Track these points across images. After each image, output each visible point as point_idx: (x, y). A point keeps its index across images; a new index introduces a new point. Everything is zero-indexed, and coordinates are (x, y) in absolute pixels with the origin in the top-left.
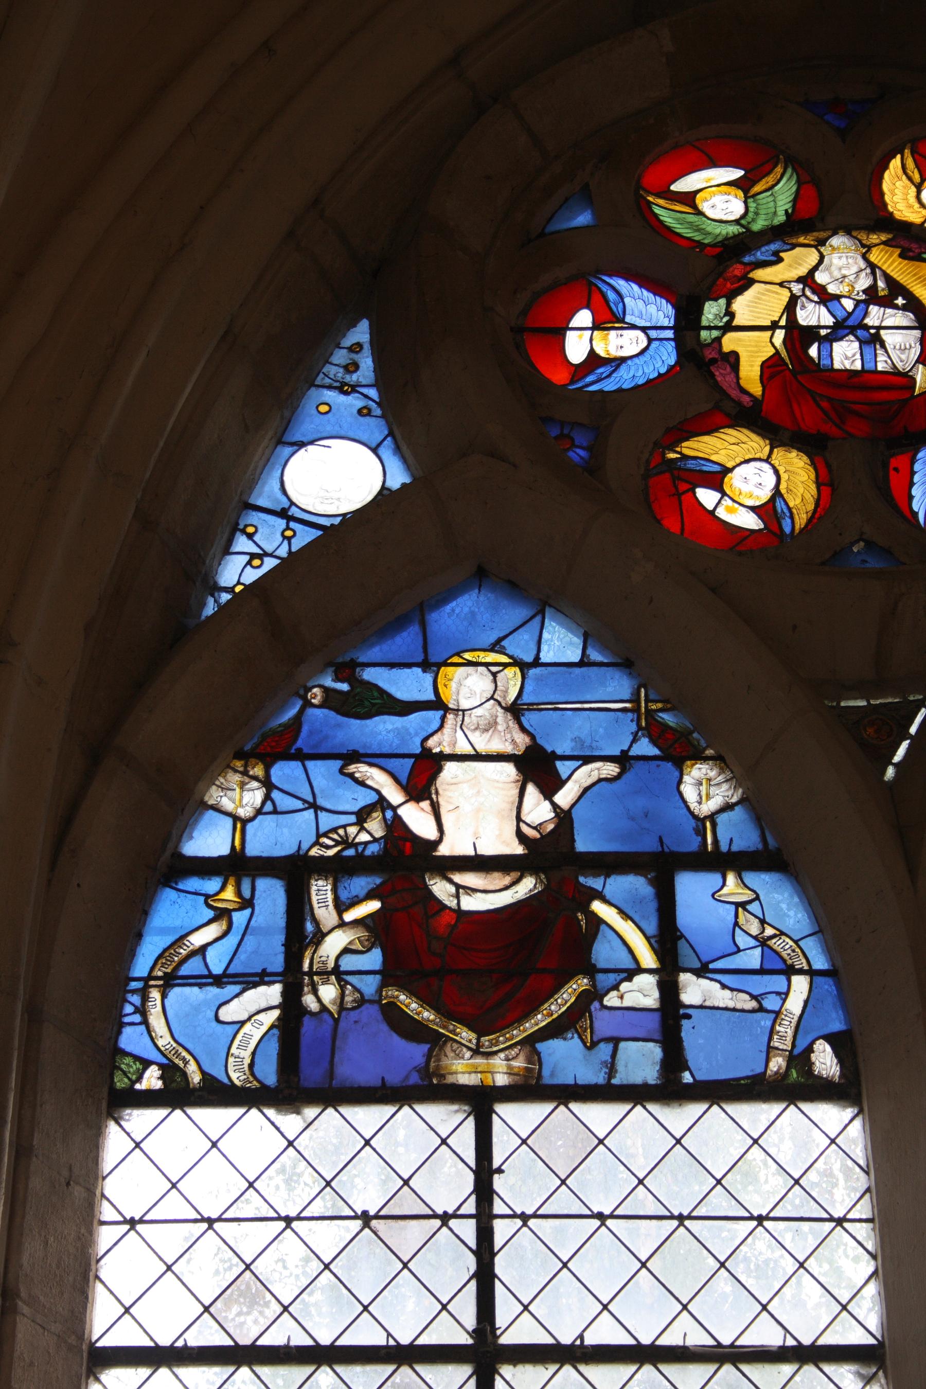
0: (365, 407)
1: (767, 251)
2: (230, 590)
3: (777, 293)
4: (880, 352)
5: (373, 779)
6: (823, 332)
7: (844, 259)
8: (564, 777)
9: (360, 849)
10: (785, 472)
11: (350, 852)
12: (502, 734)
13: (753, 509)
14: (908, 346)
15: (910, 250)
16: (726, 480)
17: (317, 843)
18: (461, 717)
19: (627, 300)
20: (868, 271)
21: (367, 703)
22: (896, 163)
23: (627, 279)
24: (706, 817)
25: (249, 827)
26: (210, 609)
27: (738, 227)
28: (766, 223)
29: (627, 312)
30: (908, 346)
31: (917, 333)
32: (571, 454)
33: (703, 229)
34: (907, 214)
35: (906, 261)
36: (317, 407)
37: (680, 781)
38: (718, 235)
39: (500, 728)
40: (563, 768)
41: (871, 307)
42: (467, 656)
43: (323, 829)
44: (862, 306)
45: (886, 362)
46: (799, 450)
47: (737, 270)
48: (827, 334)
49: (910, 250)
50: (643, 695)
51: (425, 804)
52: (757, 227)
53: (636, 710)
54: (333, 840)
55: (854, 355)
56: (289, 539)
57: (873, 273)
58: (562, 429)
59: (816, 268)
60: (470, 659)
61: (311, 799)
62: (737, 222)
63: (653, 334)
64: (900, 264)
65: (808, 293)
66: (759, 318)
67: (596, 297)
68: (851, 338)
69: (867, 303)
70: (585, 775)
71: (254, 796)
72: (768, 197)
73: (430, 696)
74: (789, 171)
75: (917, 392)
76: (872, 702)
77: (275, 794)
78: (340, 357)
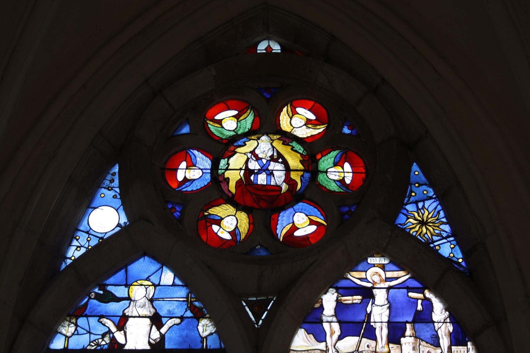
0: (115, 195)
1: (242, 141)
2: (70, 258)
3: (243, 157)
4: (272, 178)
5: (107, 323)
6: (256, 171)
7: (265, 144)
8: (164, 323)
9: (102, 346)
10: (240, 220)
11: (99, 348)
12: (147, 308)
13: (229, 232)
14: (281, 176)
15: (286, 142)
16: (222, 222)
17: (89, 345)
18: (135, 303)
19: (198, 159)
20: (272, 149)
21: (108, 298)
22: (285, 109)
23: (198, 151)
24: (204, 337)
25: (70, 339)
26: (63, 266)
27: (234, 132)
28: (242, 131)
29: (197, 163)
30: (281, 176)
31: (285, 172)
32: (175, 214)
33: (223, 133)
34: (286, 128)
35: (284, 146)
36: (100, 195)
37: (198, 325)
38: (227, 135)
39: (146, 306)
40: (164, 320)
41: (271, 162)
42: (139, 282)
43: (92, 340)
44: (268, 162)
45: (274, 182)
46: (245, 212)
47: (232, 148)
48: (257, 172)
49: (285, 141)
50: (190, 296)
51: (122, 332)
52: (239, 133)
53: (187, 301)
54: (94, 344)
55: (264, 179)
56: (89, 241)
57: (273, 150)
58: (173, 205)
59: (256, 148)
60: (140, 283)
61: (89, 330)
62: (234, 131)
63: (204, 171)
64: (282, 146)
65: (253, 157)
66: (237, 166)
67: (188, 157)
68: (264, 173)
69: (270, 161)
70: (170, 323)
71: (72, 329)
72: (244, 121)
73: (126, 296)
74: (252, 111)
75: (282, 192)
76: (258, 299)
77: (78, 328)
78: (109, 177)
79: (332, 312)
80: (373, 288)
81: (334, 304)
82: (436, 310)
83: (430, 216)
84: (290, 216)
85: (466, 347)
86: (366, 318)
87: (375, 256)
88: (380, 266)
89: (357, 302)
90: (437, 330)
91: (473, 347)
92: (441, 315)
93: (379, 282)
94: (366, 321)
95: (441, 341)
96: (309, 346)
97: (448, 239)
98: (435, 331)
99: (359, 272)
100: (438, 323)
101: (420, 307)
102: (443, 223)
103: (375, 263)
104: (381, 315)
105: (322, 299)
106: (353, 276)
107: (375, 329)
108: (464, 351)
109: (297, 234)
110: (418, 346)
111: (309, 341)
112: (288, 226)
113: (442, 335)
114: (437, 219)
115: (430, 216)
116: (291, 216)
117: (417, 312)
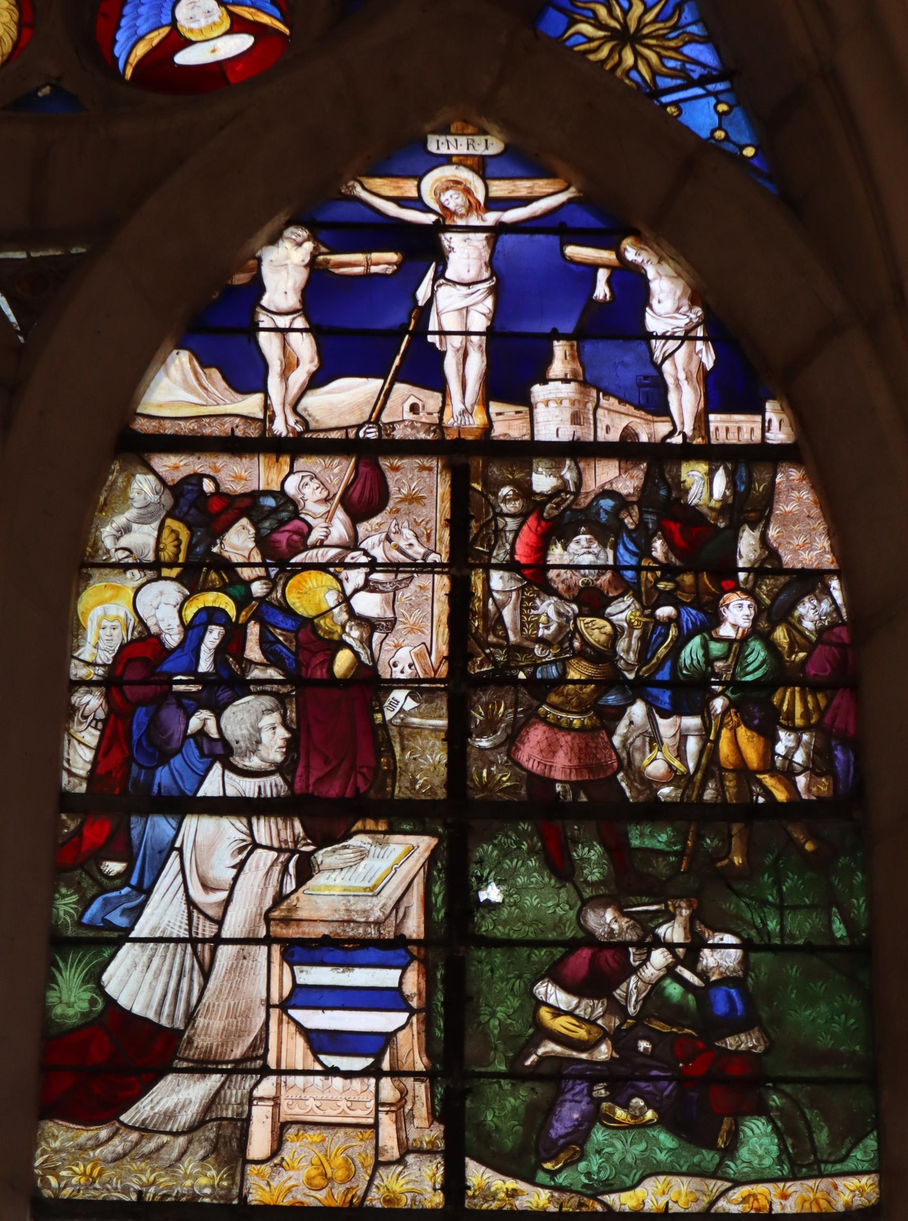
76: (33, 254)
79: (292, 301)
80: (441, 227)
81: (300, 277)
82: (659, 302)
83: (649, 17)
84: (165, 5)
85: (758, 418)
86: (410, 322)
87: (453, 130)
88: (469, 162)
89: (382, 272)
90: (659, 361)
91: (784, 416)
92: (677, 315)
93: (463, 211)
94: (411, 328)
95: (672, 397)
96: (203, 405)
97: (711, 87)
98: (654, 363)
99: (395, 180)
100: (663, 341)
101: (602, 291)
102: (693, 39)
103: (453, 151)
104: (465, 311)
105: (259, 260)
106: (375, 190)
107: (444, 354)
108: (752, 430)
109: (184, 58)
110: (591, 412)
111: (205, 389)
112: (155, 33)
113: (677, 379)
114: (674, 28)
115: (649, 17)
116: (168, 6)
117: (592, 302)
